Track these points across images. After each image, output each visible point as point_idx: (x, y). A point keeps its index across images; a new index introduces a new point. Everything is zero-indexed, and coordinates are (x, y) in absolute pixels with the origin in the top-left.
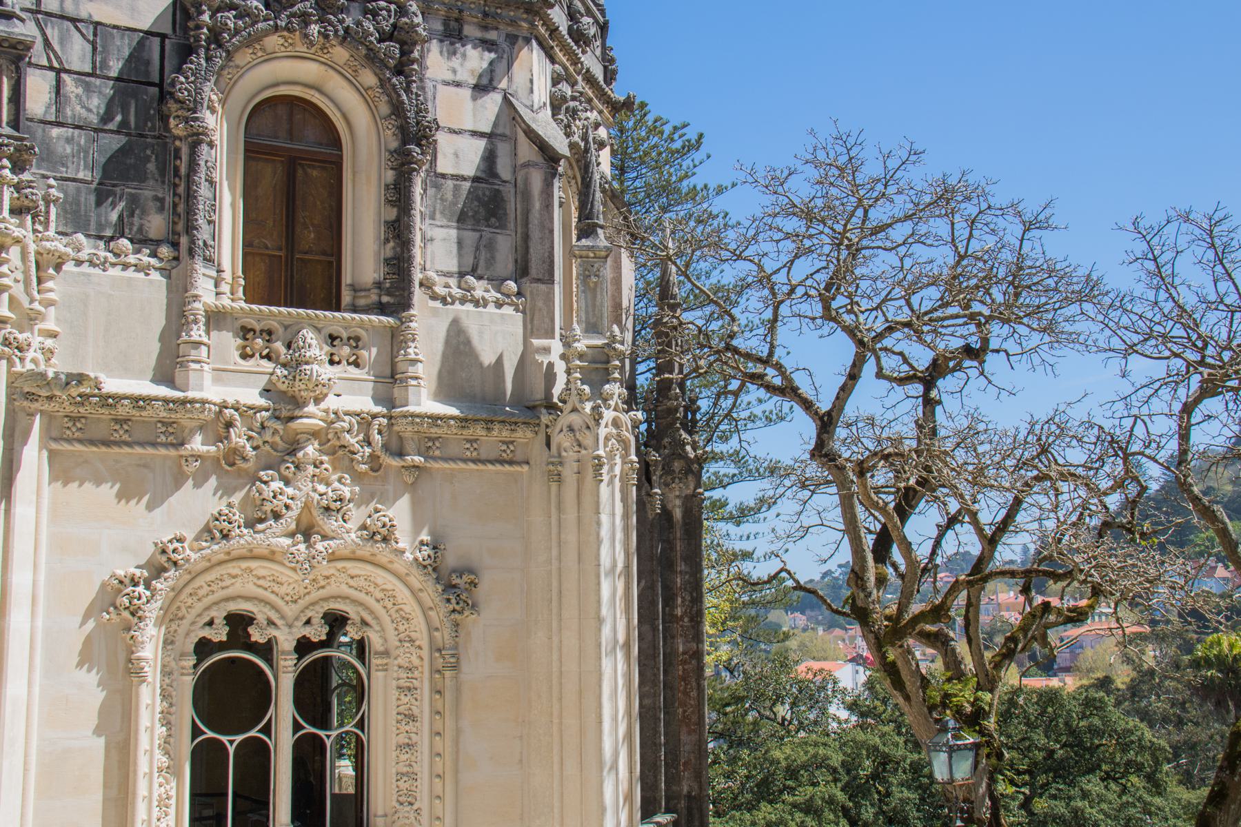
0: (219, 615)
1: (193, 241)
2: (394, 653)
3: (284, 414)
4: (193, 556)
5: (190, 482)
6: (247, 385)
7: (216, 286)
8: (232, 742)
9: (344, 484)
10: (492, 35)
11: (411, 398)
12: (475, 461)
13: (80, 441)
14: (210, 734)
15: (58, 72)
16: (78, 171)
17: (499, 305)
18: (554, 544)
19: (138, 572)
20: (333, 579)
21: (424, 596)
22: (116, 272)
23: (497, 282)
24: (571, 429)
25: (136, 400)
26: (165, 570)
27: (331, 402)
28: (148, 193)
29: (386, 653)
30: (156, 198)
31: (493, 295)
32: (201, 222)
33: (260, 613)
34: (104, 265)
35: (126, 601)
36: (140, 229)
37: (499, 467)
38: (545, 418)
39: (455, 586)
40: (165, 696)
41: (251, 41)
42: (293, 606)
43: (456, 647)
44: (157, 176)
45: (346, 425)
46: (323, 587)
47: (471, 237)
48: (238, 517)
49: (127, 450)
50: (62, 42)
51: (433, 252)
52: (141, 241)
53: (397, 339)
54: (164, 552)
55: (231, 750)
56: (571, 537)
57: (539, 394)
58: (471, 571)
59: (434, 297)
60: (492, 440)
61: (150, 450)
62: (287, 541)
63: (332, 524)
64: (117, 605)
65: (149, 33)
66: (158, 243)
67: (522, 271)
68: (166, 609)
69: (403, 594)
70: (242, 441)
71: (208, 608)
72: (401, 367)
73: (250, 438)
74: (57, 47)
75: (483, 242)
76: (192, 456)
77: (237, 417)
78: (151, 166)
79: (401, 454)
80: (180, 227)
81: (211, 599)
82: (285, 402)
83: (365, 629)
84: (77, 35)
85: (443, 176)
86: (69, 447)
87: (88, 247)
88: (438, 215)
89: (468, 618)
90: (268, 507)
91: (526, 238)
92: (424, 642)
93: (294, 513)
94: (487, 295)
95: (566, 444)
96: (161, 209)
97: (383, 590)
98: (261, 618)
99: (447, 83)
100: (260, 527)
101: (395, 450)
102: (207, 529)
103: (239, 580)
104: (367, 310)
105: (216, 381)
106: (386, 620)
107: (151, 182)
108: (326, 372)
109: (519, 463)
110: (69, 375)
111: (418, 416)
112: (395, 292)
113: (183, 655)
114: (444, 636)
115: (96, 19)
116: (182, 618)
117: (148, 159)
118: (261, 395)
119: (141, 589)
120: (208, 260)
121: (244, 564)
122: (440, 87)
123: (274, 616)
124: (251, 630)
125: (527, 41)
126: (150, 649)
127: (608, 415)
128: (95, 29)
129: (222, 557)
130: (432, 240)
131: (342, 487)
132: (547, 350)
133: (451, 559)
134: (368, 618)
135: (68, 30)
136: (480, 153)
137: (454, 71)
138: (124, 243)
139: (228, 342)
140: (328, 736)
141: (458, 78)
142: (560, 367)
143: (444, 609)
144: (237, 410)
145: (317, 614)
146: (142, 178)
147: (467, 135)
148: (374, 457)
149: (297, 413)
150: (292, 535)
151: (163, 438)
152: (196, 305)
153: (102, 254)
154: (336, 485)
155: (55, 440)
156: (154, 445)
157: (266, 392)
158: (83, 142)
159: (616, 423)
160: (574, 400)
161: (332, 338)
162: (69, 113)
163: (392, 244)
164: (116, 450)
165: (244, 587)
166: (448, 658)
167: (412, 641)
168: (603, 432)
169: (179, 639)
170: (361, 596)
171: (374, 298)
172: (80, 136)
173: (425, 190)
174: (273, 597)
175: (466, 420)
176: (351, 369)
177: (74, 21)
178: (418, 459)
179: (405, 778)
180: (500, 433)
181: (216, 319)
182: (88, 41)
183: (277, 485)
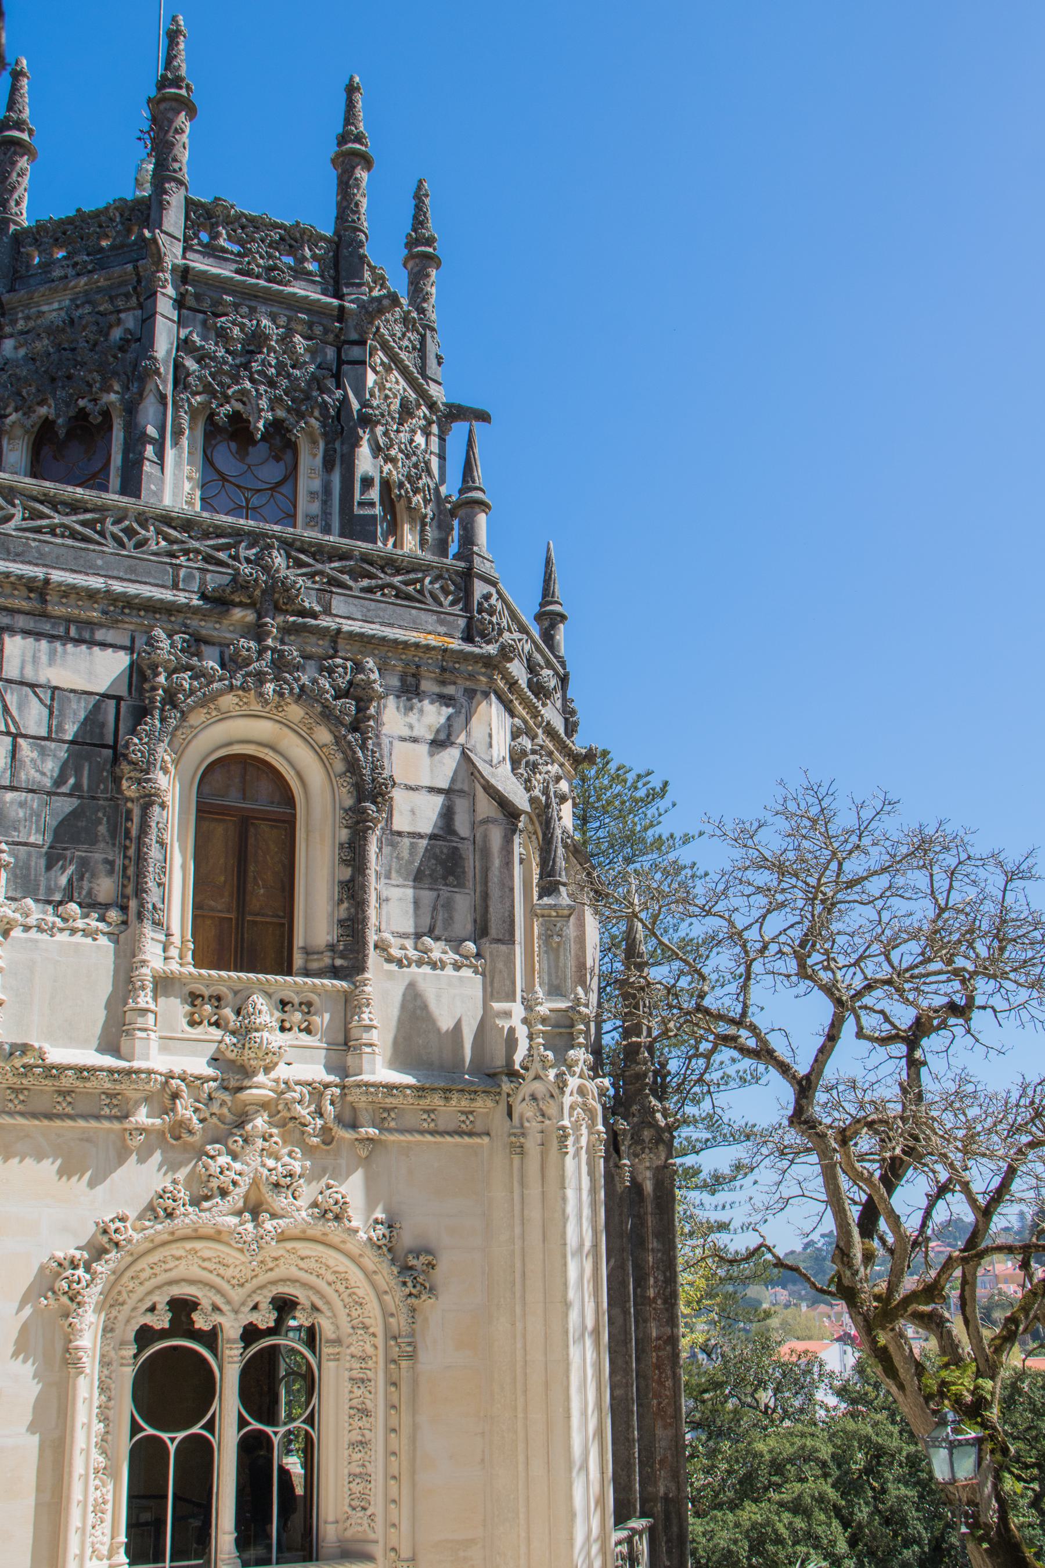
0: (161, 1299)
1: (142, 905)
2: (346, 1341)
3: (233, 1084)
4: (136, 1237)
5: (134, 1157)
6: (194, 1054)
7: (165, 951)
8: (172, 1440)
9: (294, 1158)
10: (450, 690)
11: (366, 1066)
12: (432, 1133)
13: (22, 1114)
14: (150, 1431)
15: (15, 737)
16: (29, 835)
17: (457, 967)
18: (517, 1221)
19: (78, 1254)
20: (282, 1260)
21: (378, 1278)
22: (63, 937)
23: (456, 944)
24: (534, 1098)
25: (80, 1070)
26: (106, 1251)
27: (282, 1071)
28: (98, 856)
29: (338, 1342)
30: (106, 861)
31: (451, 956)
32: (151, 884)
33: (205, 1297)
34: (51, 930)
35: (65, 1285)
36: (90, 893)
37: (458, 1139)
38: (506, 1086)
39: (411, 1268)
40: (103, 1389)
41: (206, 701)
42: (240, 1290)
43: (412, 1334)
44: (108, 839)
45: (297, 1096)
46: (271, 1270)
47: (427, 896)
48: (183, 1195)
49: (70, 1123)
50: (20, 708)
51: (388, 913)
52: (90, 905)
53: (350, 1005)
54: (105, 1232)
55: (172, 1448)
56: (535, 1214)
57: (500, 1061)
58: (429, 1252)
59: (390, 960)
60: (450, 1110)
61: (94, 1124)
62: (234, 1220)
63: (281, 1201)
64: (55, 1290)
65: (105, 696)
66: (107, 906)
67: (481, 931)
68: (106, 1294)
69: (356, 1276)
70: (189, 1113)
71: (150, 1293)
72: (355, 1033)
73: (196, 1110)
75: (441, 901)
76: (136, 1129)
77: (184, 1087)
78: (102, 829)
79: (354, 1126)
80: (129, 890)
81: (154, 1282)
82: (234, 1072)
83: (316, 1314)
84: (35, 700)
85: (399, 834)
86: (12, 1121)
87: (36, 912)
88: (394, 875)
89: (426, 1303)
90: (214, 1183)
91: (485, 896)
92: (379, 1330)
93: (241, 1190)
94: (444, 957)
95: (529, 1114)
96: (111, 872)
97: (335, 1272)
98: (205, 1303)
99: (403, 739)
100: (206, 1205)
101: (349, 1120)
102: (151, 1208)
103: (183, 1262)
104: (319, 974)
105: (163, 1049)
106: (338, 1304)
107: (102, 845)
108: (276, 1039)
109: (479, 1135)
110: (14, 1046)
111: (372, 1085)
112: (349, 956)
113: (123, 1343)
114: (400, 1322)
115: (54, 683)
116: (122, 1304)
117: (99, 822)
118: (209, 1064)
119: (80, 1272)
120: (157, 924)
121: (189, 1245)
122: (397, 744)
123: (219, 1301)
124: (195, 1316)
125: (486, 695)
126: (89, 1337)
127: (573, 1082)
128: (53, 693)
129: (166, 1237)
131: (292, 1161)
132: (508, 1014)
133: (407, 1239)
134: (319, 1303)
135: (27, 696)
136: (437, 809)
137: (411, 727)
138: (73, 907)
139: (175, 1008)
140: (276, 1433)
141: (415, 733)
142: (522, 1032)
143: (400, 1292)
144: (183, 1080)
145: (264, 1299)
146: (93, 841)
147: (424, 792)
148: (325, 1130)
149: (246, 1083)
150: (239, 1213)
151: (107, 1111)
152: (144, 970)
153: (51, 919)
154: (286, 1159)
156: (98, 1117)
157: (214, 1060)
158: (35, 806)
159: (581, 1091)
160: (536, 1067)
161: (284, 1003)
162: (23, 777)
163: (346, 905)
164: (58, 1123)
165: (188, 1270)
166: (404, 1347)
167: (366, 1328)
168: (567, 1100)
169: (119, 1326)
170: (312, 1279)
171: (327, 961)
172: (33, 800)
173: (380, 849)
174: (218, 1281)
175: (423, 1089)
176: (303, 1036)
177: (33, 686)
178: (372, 1131)
179: (358, 1480)
180: (459, 1102)
181: (163, 984)
182: (45, 705)
183: (224, 1160)
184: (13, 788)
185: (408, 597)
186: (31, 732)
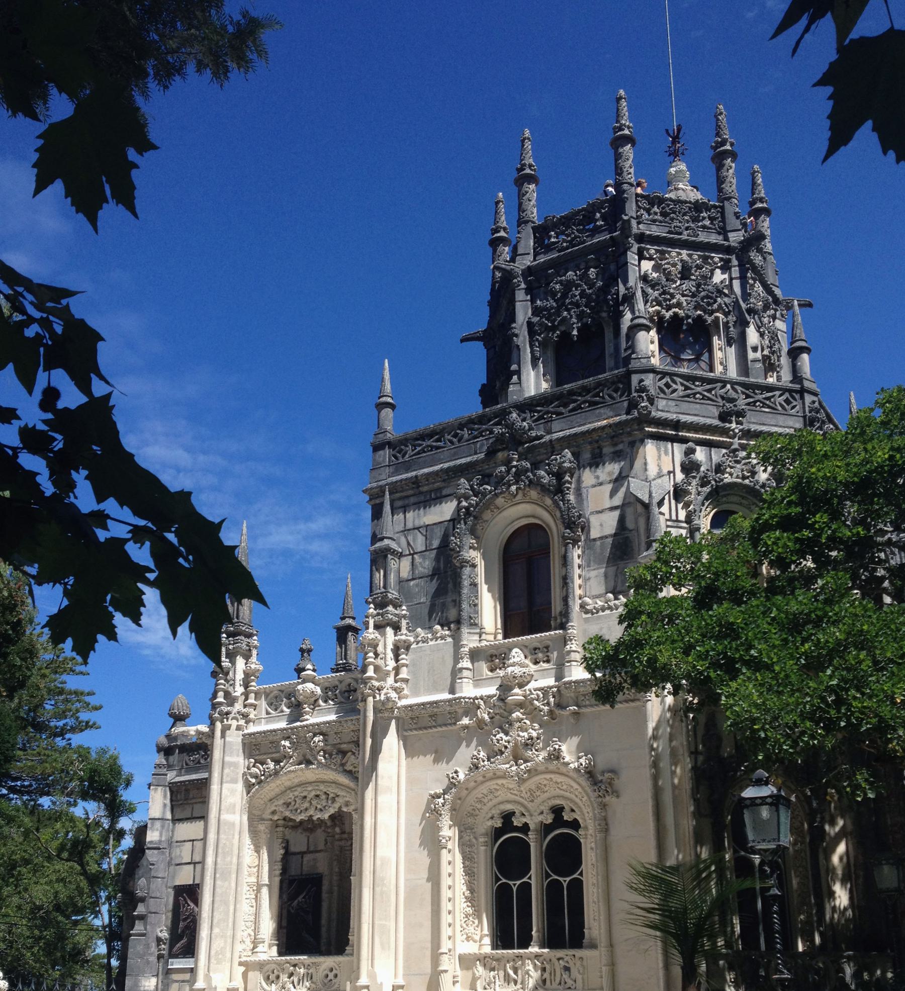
5: (464, 744)
10: (620, 447)
13: (416, 729)
14: (504, 881)
28: (449, 599)
33: (517, 809)
41: (487, 506)
47: (612, 570)
50: (414, 540)
61: (444, 728)
65: (449, 521)
74: (412, 543)
85: (594, 540)
88: (592, 564)
107: (450, 594)
117: (448, 582)
125: (642, 441)
130: (589, 579)
136: (617, 519)
144: (482, 699)
148: (551, 712)
155: (406, 730)
156: (445, 725)
177: (418, 528)
184: (413, 579)
185: (596, 403)
186: (419, 550)
